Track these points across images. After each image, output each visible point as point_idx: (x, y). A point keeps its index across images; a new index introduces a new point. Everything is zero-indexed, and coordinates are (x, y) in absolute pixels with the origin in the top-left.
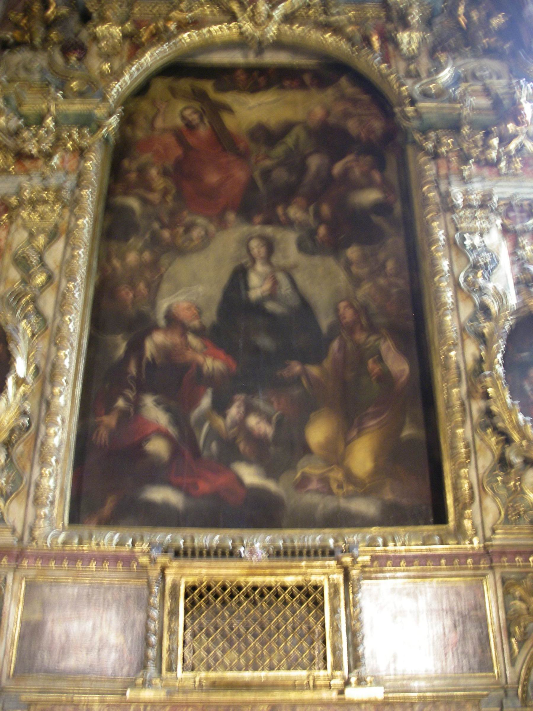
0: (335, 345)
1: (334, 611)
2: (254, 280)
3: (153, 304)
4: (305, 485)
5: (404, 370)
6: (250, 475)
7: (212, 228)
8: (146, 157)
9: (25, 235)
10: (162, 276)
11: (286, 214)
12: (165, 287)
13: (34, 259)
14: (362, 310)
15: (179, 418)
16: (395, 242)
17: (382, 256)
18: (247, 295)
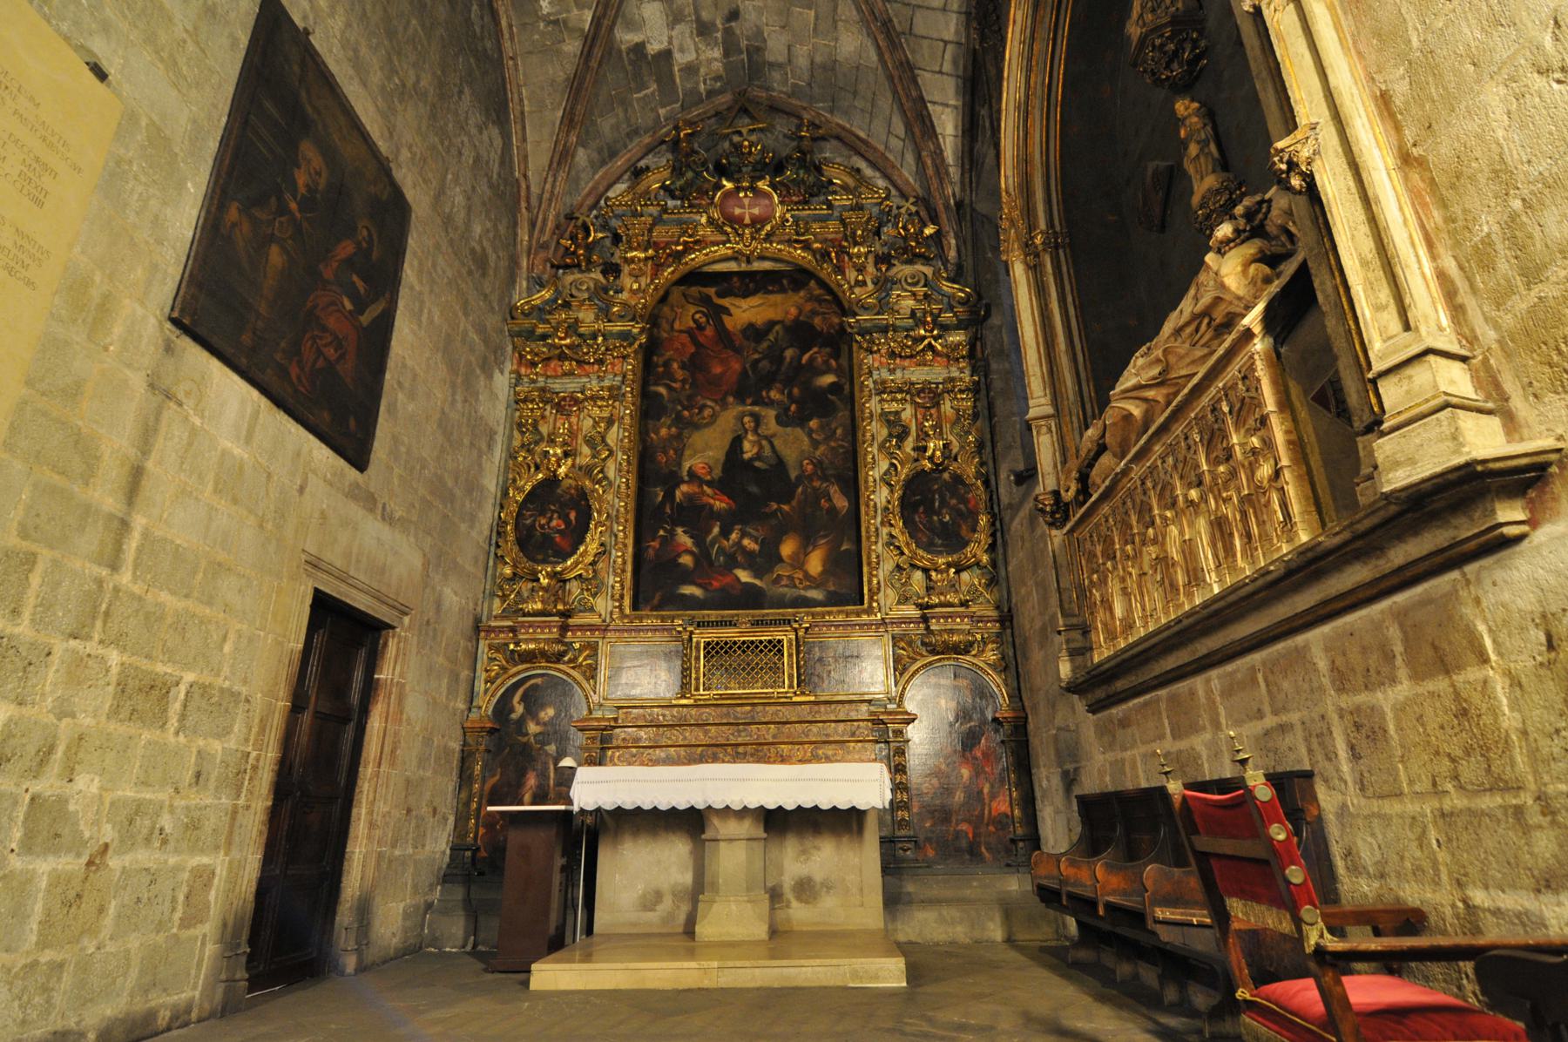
1: (790, 655)
2: (746, 445)
3: (680, 465)
4: (780, 582)
6: (744, 576)
8: (669, 354)
9: (590, 422)
12: (687, 453)
13: (599, 439)
14: (818, 464)
15: (699, 539)
16: (843, 414)
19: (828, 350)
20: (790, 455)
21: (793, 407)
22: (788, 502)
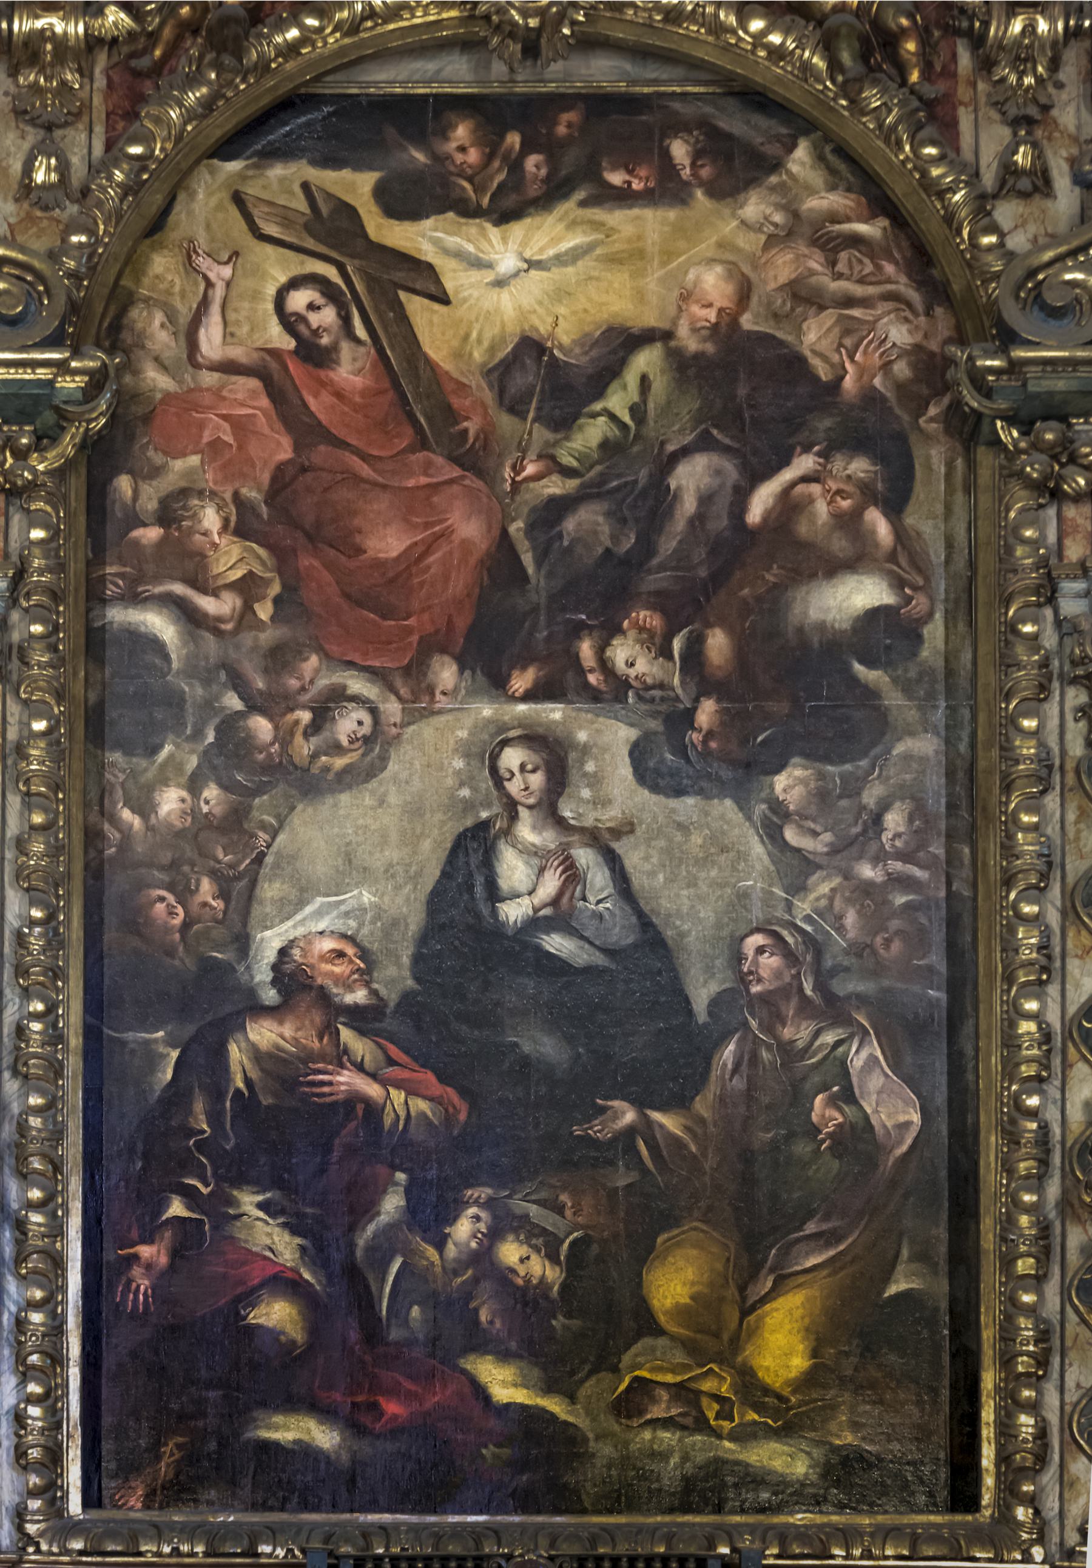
0: (730, 1049)
2: (512, 868)
3: (243, 943)
5: (907, 1124)
6: (503, 1383)
7: (392, 709)
10: (259, 859)
11: (605, 666)
12: (270, 890)
17: (871, 796)
18: (494, 912)
19: (860, 467)
20: (690, 911)
21: (707, 713)
22: (679, 1102)
